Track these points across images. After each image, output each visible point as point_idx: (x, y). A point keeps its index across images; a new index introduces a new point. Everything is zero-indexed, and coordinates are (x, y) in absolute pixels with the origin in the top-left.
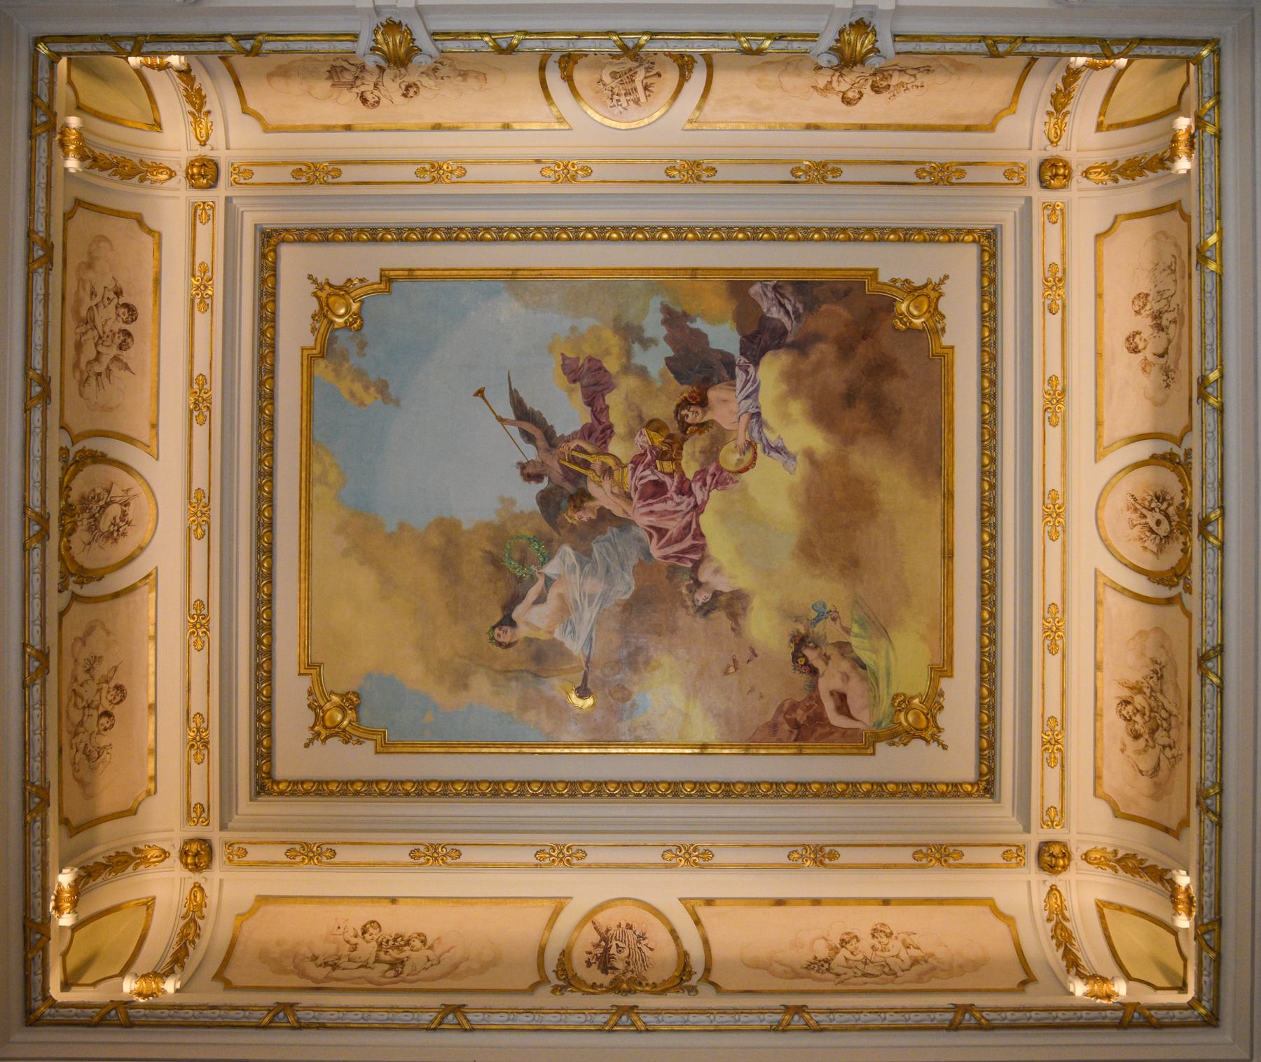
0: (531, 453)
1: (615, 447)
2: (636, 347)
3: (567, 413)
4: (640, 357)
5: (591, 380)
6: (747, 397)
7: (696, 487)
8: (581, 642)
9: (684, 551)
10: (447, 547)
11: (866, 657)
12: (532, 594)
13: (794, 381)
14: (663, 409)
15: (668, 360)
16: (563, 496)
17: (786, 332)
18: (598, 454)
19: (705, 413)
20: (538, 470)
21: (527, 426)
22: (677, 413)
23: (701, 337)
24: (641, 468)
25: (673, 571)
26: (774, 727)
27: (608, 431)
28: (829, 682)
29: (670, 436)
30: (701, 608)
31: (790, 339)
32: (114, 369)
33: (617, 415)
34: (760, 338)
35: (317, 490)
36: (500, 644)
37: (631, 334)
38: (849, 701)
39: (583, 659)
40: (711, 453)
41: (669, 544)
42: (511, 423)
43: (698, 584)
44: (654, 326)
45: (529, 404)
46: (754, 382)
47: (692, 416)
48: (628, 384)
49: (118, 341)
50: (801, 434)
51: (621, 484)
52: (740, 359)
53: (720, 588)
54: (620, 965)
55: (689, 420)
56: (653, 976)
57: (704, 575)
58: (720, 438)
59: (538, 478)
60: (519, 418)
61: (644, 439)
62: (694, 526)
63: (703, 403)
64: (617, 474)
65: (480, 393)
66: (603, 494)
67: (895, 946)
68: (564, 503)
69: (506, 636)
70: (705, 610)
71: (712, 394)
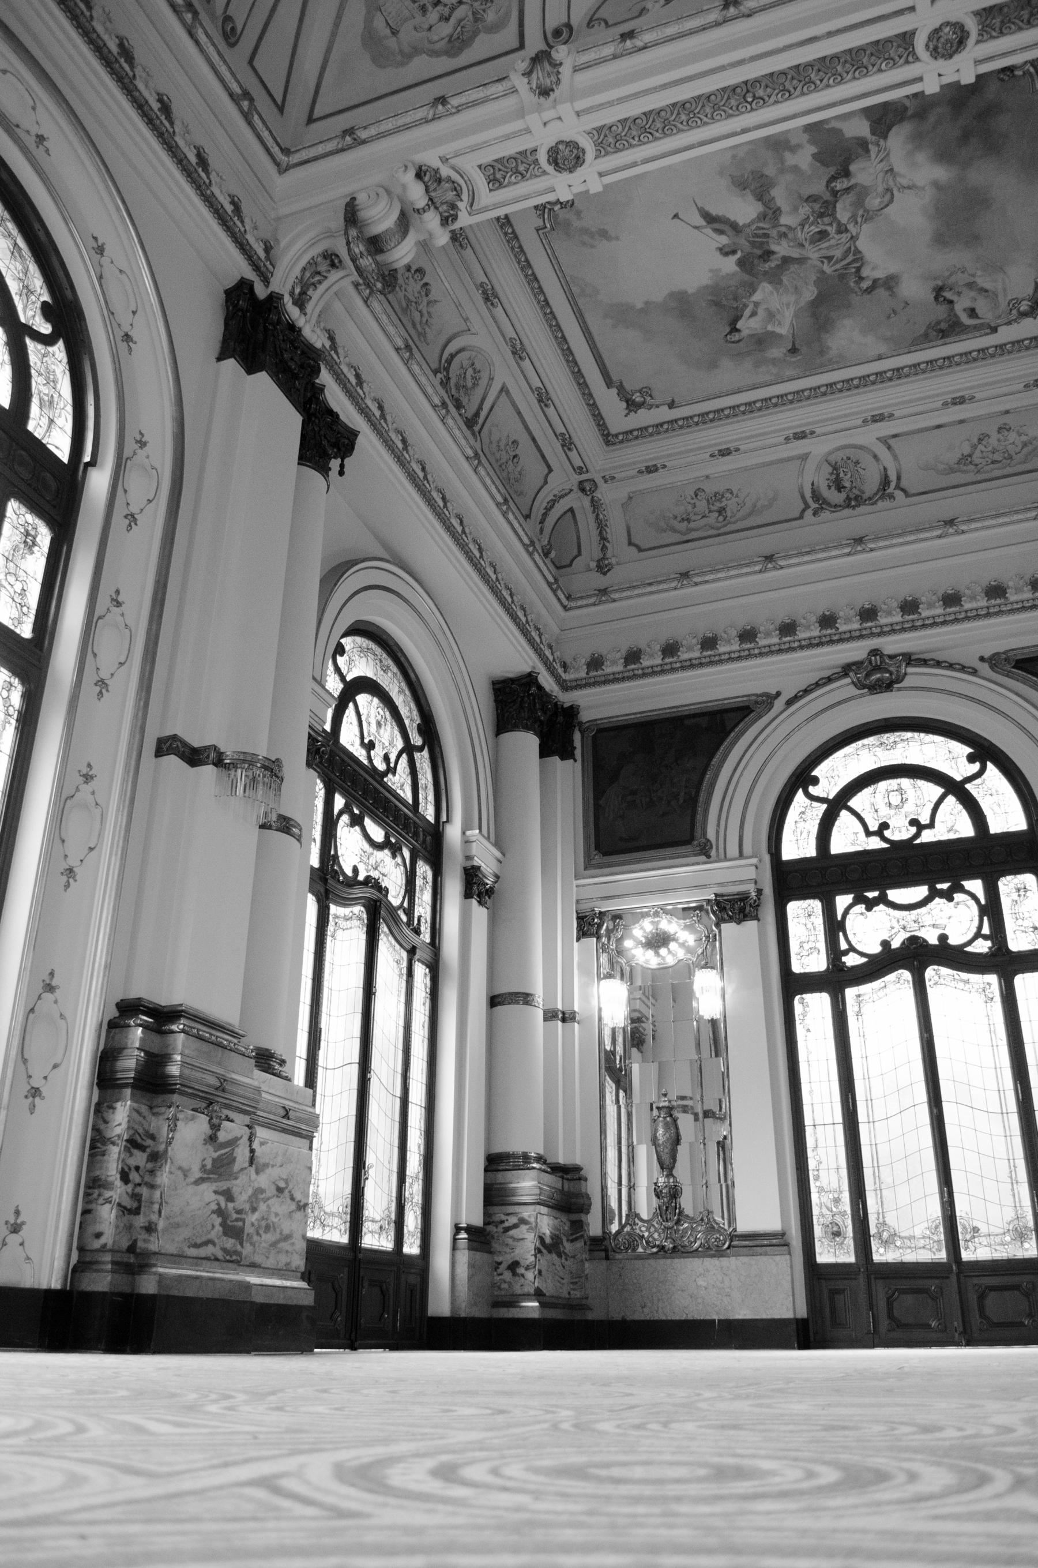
0: (724, 240)
1: (784, 220)
2: (787, 155)
3: (744, 210)
4: (790, 159)
6: (882, 161)
7: (850, 227)
8: (786, 328)
9: (849, 264)
10: (681, 305)
11: (987, 285)
12: (747, 312)
13: (917, 139)
14: (818, 187)
15: (814, 156)
17: (906, 109)
18: (773, 227)
19: (849, 181)
20: (733, 248)
21: (717, 226)
22: (827, 187)
24: (807, 226)
25: (842, 277)
27: (777, 212)
29: (826, 202)
30: (866, 290)
31: (910, 113)
32: (431, 309)
36: (733, 342)
38: (977, 311)
39: (790, 336)
40: (859, 203)
41: (837, 262)
42: (705, 227)
43: (861, 279)
45: (714, 211)
46: (885, 150)
47: (839, 185)
49: (423, 294)
51: (795, 239)
53: (878, 277)
54: (847, 484)
55: (838, 188)
57: (865, 272)
58: (861, 193)
59: (734, 252)
60: (709, 223)
61: (805, 210)
62: (853, 249)
63: (847, 174)
64: (790, 235)
65: (676, 216)
66: (782, 249)
68: (756, 261)
69: (736, 337)
70: (869, 290)
71: (853, 168)
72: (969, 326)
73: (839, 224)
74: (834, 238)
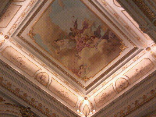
0: (73, 27)
1: (82, 35)
2: (93, 27)
3: (80, 27)
5: (86, 26)
10: (56, 28)
12: (61, 41)
13: (105, 44)
14: (90, 35)
16: (72, 35)
23: (100, 32)
26: (73, 70)
27: (82, 32)
28: (81, 71)
33: (85, 32)
34: (106, 37)
35: (47, 11)
37: (94, 25)
40: (90, 43)
43: (77, 53)
44: (97, 26)
45: (77, 23)
47: (92, 38)
48: (89, 30)
50: (100, 49)
52: (102, 37)
56: (44, 83)
57: (79, 53)
58: (92, 42)
59: (72, 31)
61: (85, 36)
64: (79, 37)
65: (73, 17)
66: (76, 38)
67: (67, 95)
69: (55, 42)
70: (76, 56)
71: (96, 38)
72: (78, 74)
73: (85, 43)
74: (82, 45)
